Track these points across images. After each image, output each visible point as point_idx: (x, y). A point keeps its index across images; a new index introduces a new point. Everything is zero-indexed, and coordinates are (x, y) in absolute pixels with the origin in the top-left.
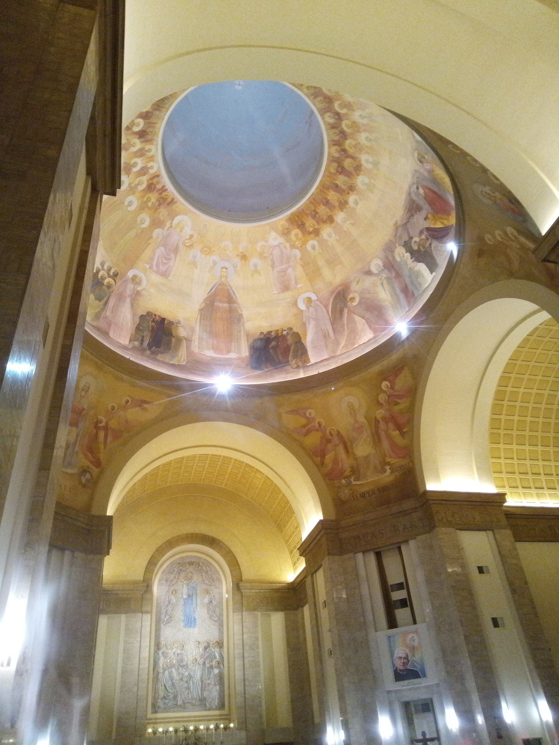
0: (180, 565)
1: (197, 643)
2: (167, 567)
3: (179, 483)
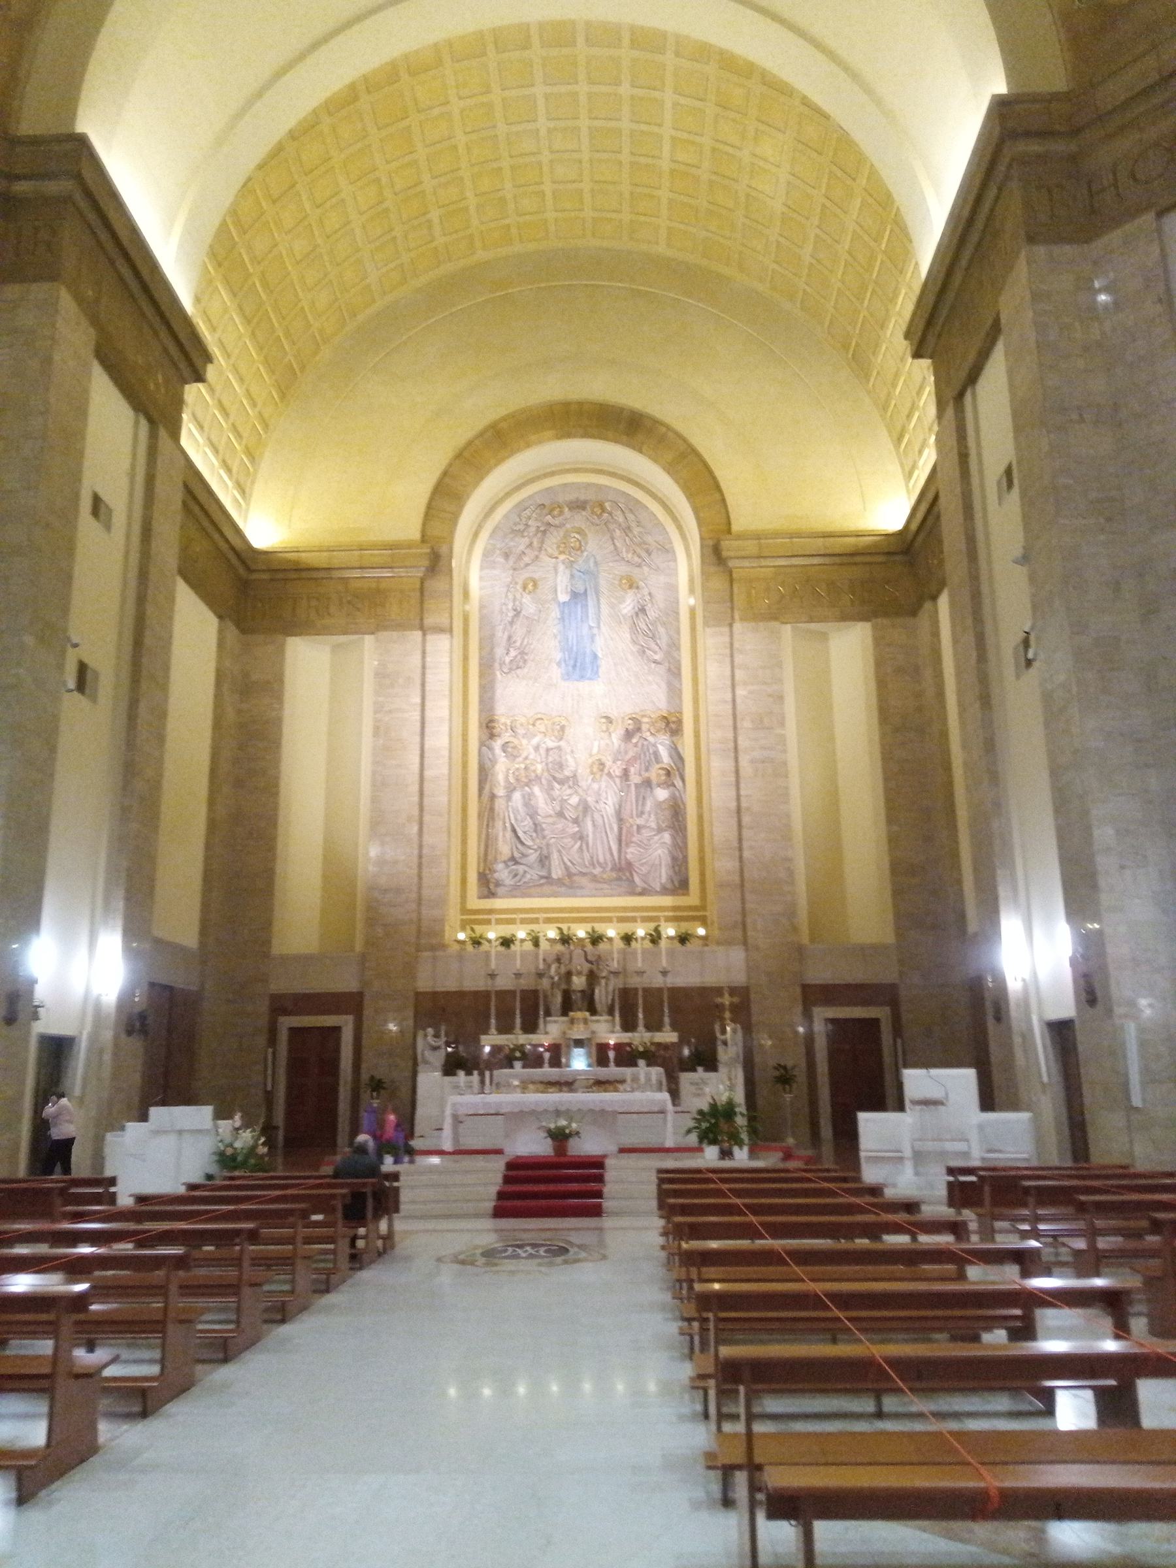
0: (545, 511)
1: (663, 772)
2: (506, 516)
3: (518, 248)
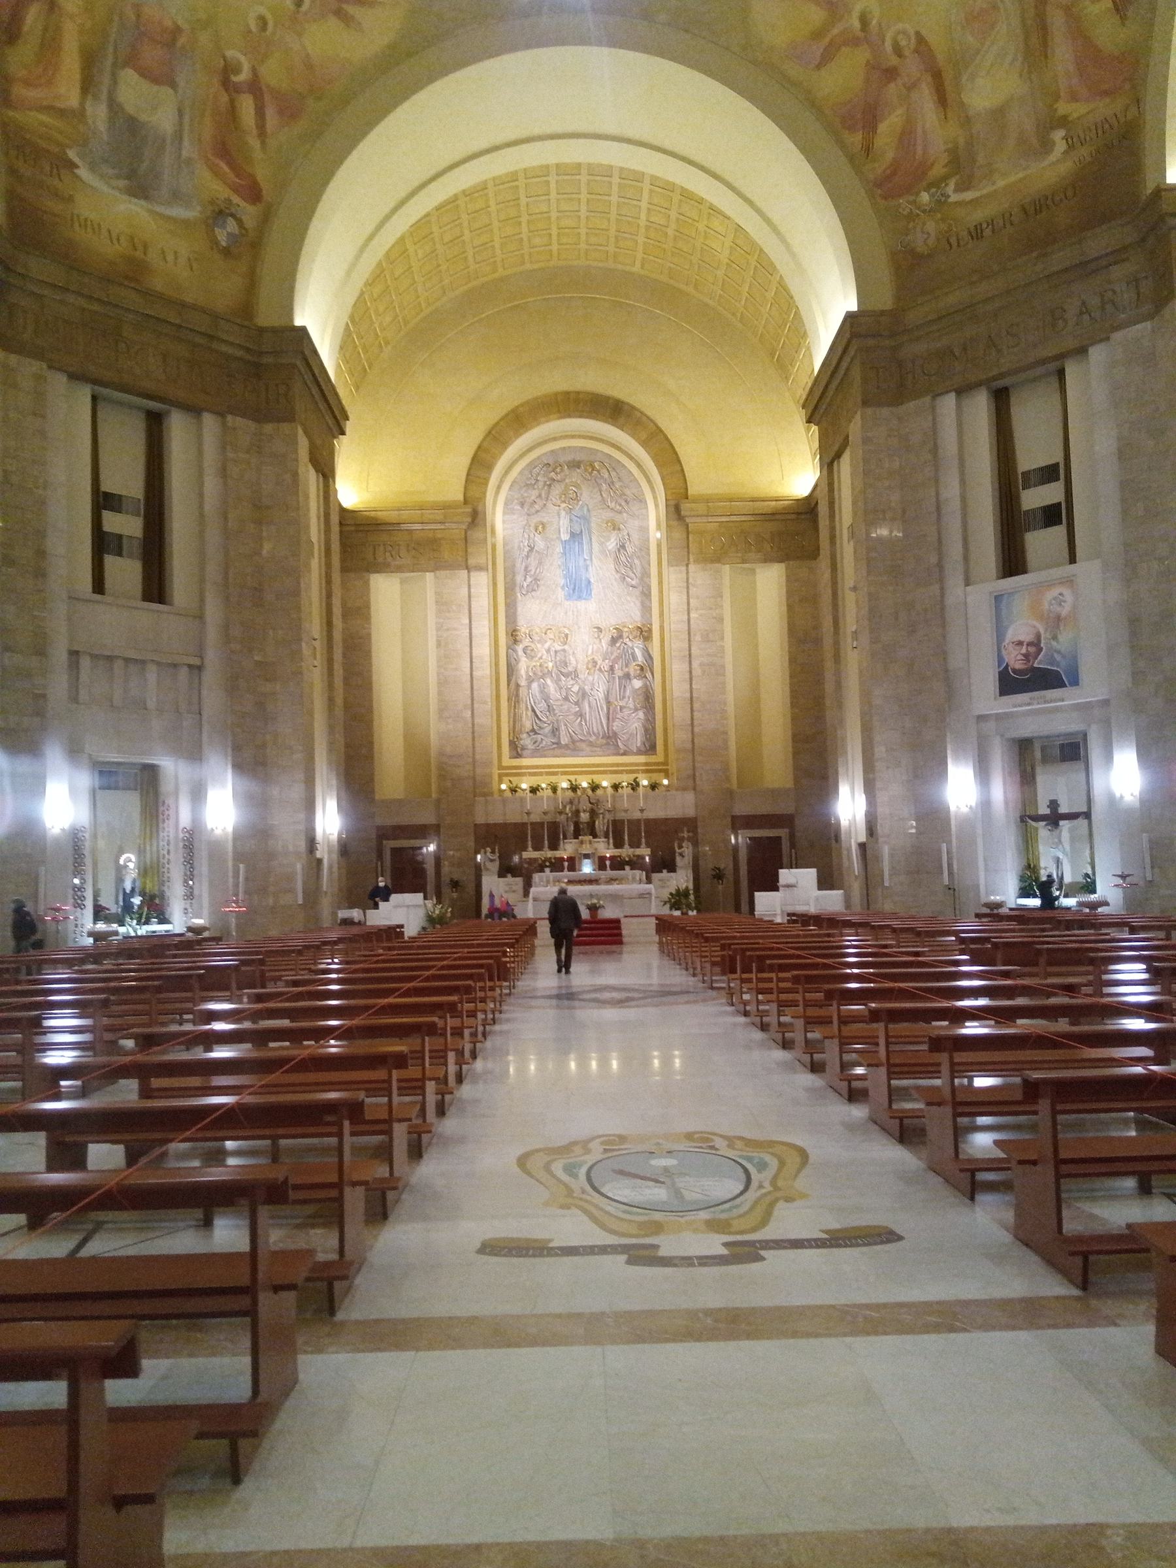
0: (550, 469)
2: (521, 473)
